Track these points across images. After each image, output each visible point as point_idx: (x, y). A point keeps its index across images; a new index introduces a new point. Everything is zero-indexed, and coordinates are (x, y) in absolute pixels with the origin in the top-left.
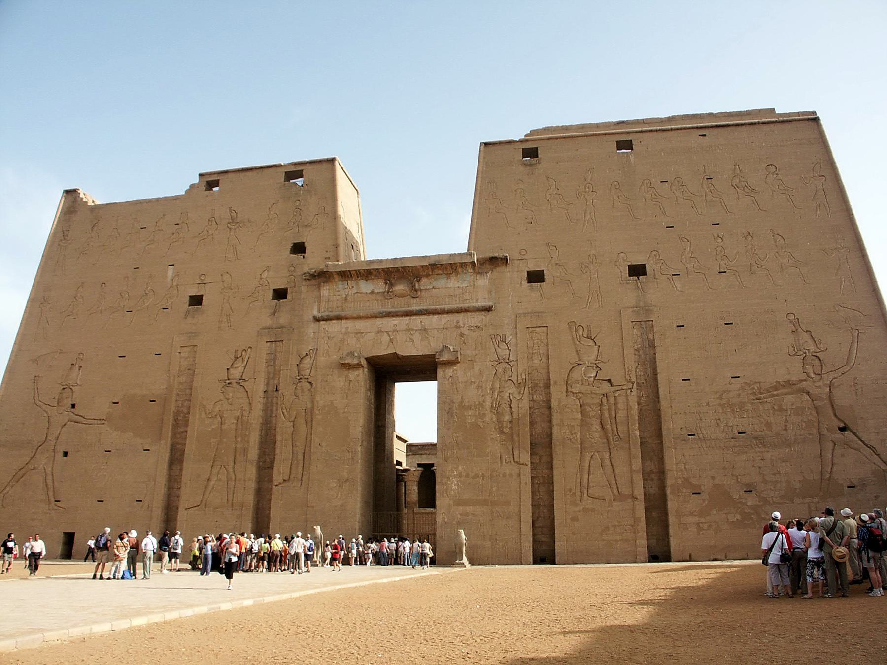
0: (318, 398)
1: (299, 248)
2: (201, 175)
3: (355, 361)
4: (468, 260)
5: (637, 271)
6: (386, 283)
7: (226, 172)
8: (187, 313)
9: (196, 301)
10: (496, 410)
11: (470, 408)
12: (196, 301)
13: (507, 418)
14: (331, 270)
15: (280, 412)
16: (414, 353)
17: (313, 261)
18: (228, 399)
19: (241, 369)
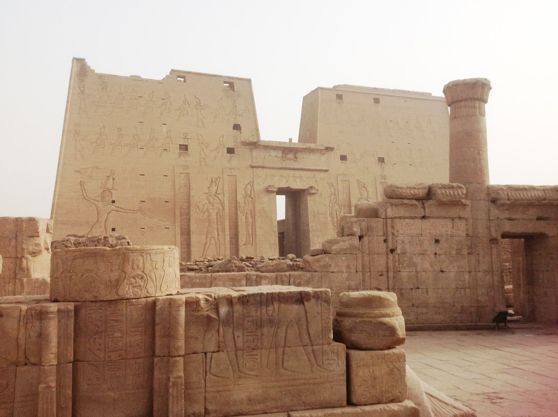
0: (256, 205)
1: (237, 127)
2: (172, 71)
3: (276, 190)
4: (322, 148)
5: (381, 160)
6: (283, 153)
7: (189, 73)
8: (180, 154)
9: (184, 148)
10: (331, 214)
11: (321, 214)
12: (184, 148)
13: (336, 219)
14: (262, 144)
15: (239, 211)
16: (297, 188)
17: (246, 135)
18: (210, 203)
19: (216, 188)
